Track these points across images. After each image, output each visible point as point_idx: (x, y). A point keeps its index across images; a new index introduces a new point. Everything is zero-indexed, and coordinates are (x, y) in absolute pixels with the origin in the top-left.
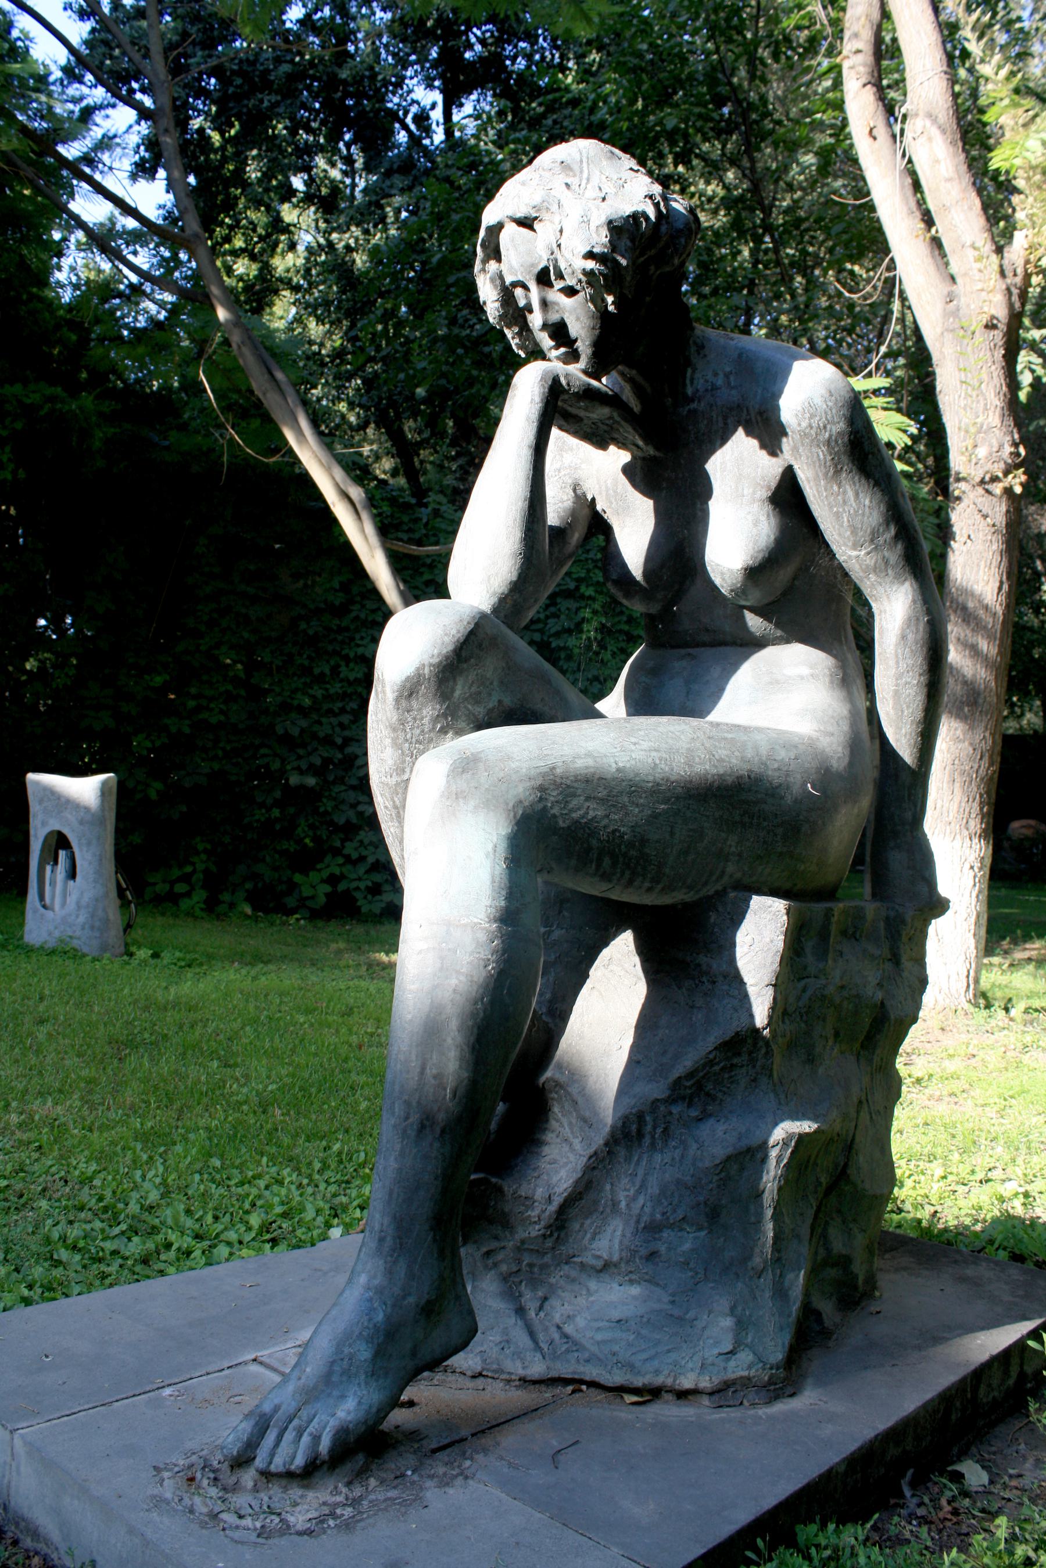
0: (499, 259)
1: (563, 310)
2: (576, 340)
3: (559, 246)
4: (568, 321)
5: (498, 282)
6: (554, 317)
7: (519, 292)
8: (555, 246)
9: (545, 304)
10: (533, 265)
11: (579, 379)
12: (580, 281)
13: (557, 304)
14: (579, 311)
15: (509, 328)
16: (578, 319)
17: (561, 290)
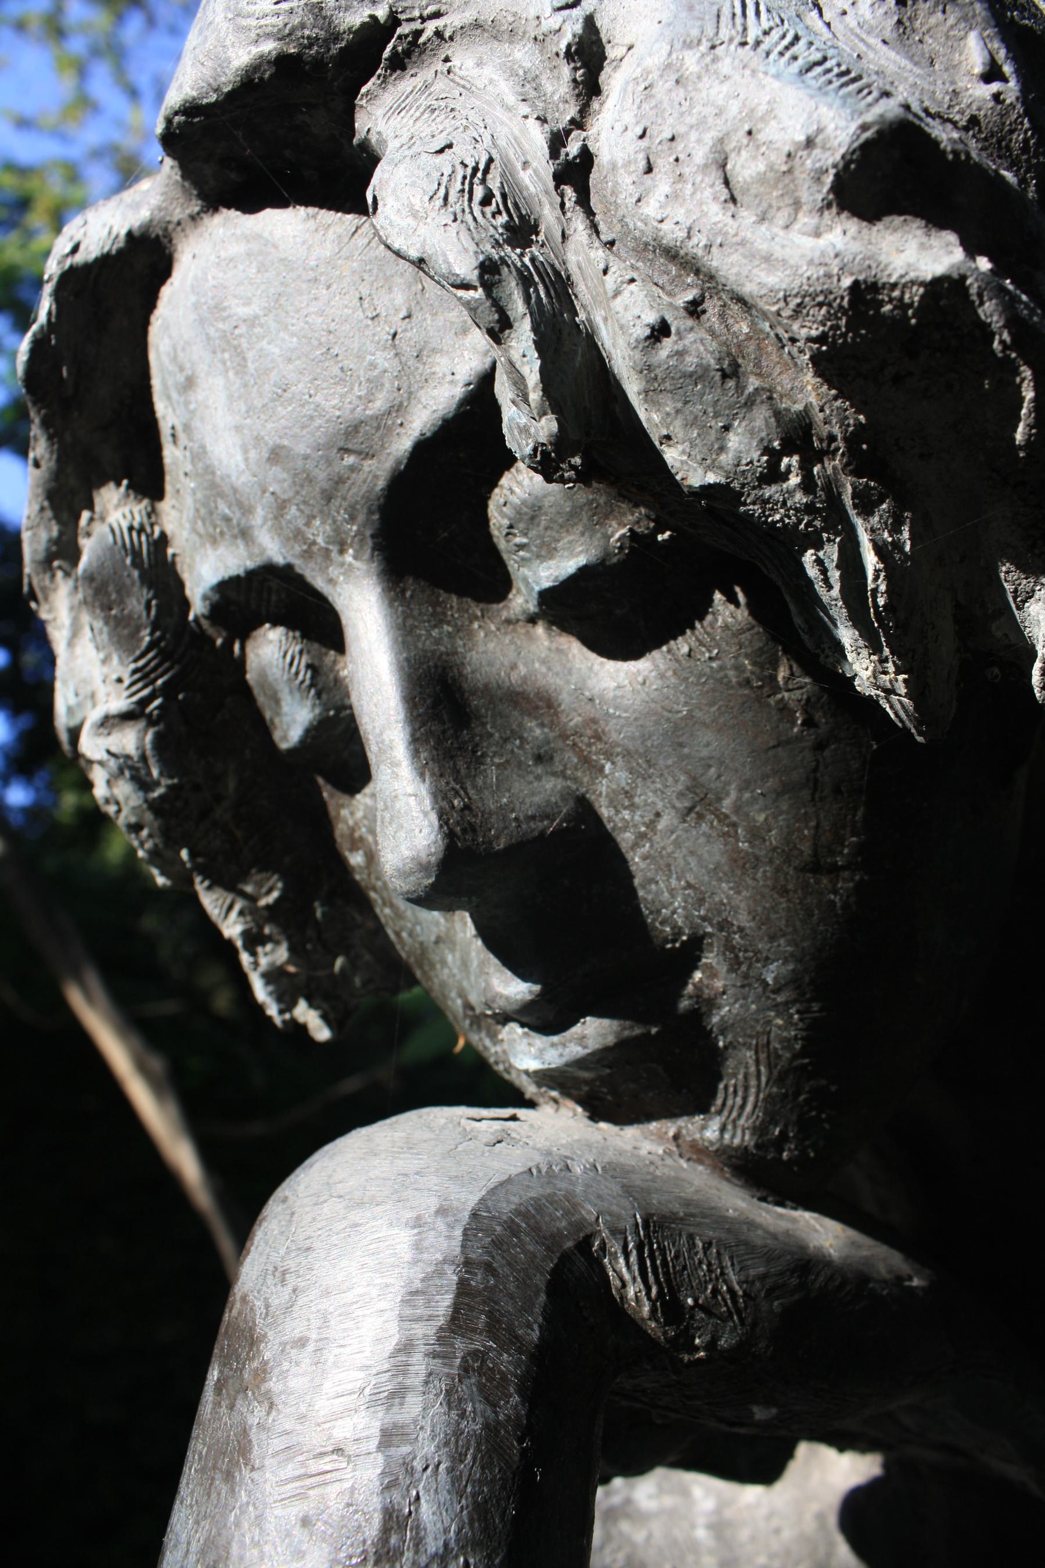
0: (149, 483)
1: (589, 742)
2: (691, 952)
3: (575, 173)
4: (623, 823)
5: (138, 602)
6: (526, 797)
7: (271, 650)
8: (535, 177)
9: (448, 709)
10: (354, 438)
11: (736, 1239)
12: (797, 436)
13: (539, 703)
14: (707, 743)
15: (227, 880)
16: (699, 803)
17: (562, 607)
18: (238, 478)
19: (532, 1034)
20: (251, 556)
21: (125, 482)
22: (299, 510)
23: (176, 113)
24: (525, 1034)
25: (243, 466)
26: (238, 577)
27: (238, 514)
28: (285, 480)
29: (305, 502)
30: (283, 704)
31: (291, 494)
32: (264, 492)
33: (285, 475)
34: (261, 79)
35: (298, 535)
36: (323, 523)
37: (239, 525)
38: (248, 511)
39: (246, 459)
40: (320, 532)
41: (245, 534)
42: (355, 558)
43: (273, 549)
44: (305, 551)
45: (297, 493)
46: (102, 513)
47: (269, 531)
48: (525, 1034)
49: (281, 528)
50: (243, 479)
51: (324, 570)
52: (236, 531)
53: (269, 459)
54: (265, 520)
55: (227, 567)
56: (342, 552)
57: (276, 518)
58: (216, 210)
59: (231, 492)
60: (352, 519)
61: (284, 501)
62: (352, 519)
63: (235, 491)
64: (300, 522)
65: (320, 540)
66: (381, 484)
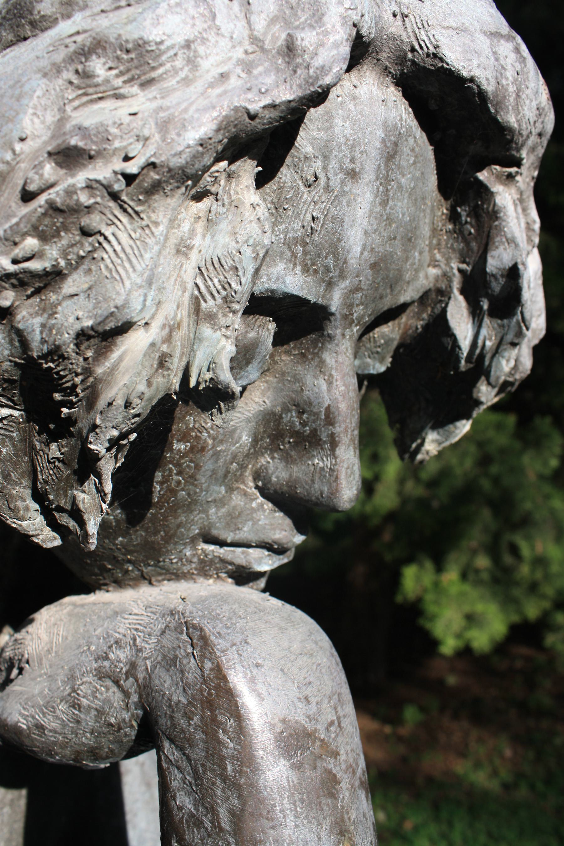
18: (352, 258)
19: (273, 555)
20: (324, 296)
21: (260, 169)
22: (362, 297)
23: (478, 86)
24: (269, 555)
25: (358, 255)
26: (308, 301)
27: (337, 273)
28: (369, 280)
29: (366, 296)
30: (251, 365)
31: (366, 288)
32: (357, 276)
33: (371, 278)
34: (506, 135)
35: (350, 306)
36: (363, 309)
37: (331, 278)
38: (342, 276)
39: (362, 253)
40: (358, 312)
41: (330, 285)
42: (357, 331)
43: (335, 302)
44: (346, 315)
45: (368, 290)
46: (234, 172)
47: (342, 294)
48: (269, 555)
49: (348, 298)
50: (353, 261)
51: (345, 328)
52: (327, 279)
53: (371, 264)
54: (346, 288)
55: (309, 292)
56: (356, 325)
57: (350, 291)
58: (397, 84)
59: (342, 261)
60: (369, 316)
61: (361, 288)
62: (369, 316)
63: (345, 262)
64: (357, 302)
65: (355, 315)
66: (385, 308)
